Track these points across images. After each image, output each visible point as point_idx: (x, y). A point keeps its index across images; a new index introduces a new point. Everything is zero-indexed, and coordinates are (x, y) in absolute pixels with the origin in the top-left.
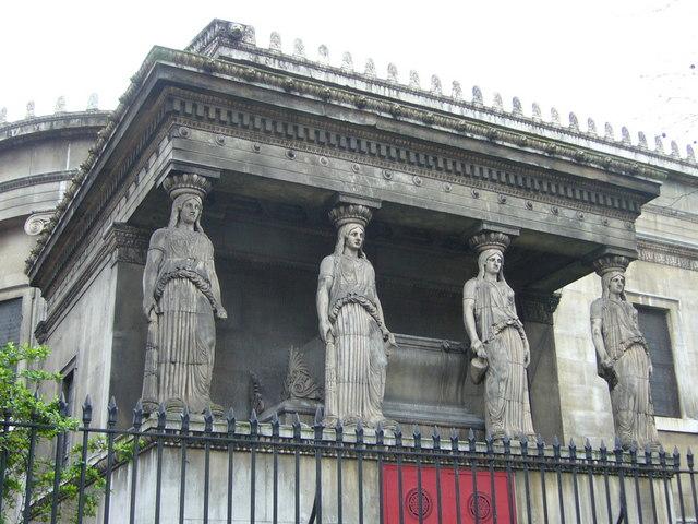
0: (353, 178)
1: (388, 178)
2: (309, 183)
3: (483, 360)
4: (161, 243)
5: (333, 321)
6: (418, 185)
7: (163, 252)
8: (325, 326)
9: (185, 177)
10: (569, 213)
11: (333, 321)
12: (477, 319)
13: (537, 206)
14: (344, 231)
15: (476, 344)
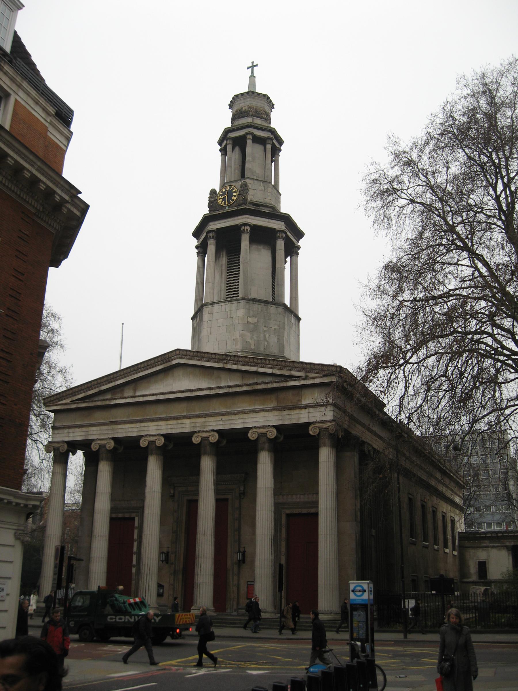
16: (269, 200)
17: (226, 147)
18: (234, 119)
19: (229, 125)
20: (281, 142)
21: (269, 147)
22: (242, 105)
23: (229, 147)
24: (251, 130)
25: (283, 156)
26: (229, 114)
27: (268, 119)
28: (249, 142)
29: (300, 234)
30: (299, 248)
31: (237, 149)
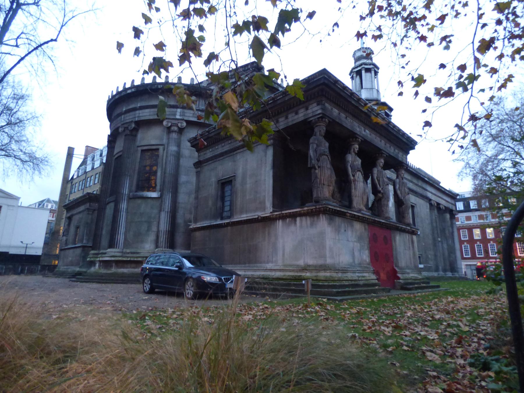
0: (358, 129)
1: (365, 131)
2: (349, 128)
3: (382, 194)
4: (316, 142)
5: (354, 176)
6: (370, 135)
7: (317, 145)
8: (352, 178)
9: (324, 119)
10: (397, 151)
11: (354, 176)
12: (379, 181)
13: (392, 147)
14: (353, 147)
15: (380, 189)
16: (375, 96)
17: (353, 76)
18: (355, 63)
19: (353, 65)
20: (378, 69)
21: (373, 72)
22: (359, 54)
23: (355, 75)
24: (363, 66)
25: (379, 75)
26: (353, 61)
27: (371, 59)
28: (363, 72)
29: (391, 110)
30: (391, 116)
31: (358, 77)
